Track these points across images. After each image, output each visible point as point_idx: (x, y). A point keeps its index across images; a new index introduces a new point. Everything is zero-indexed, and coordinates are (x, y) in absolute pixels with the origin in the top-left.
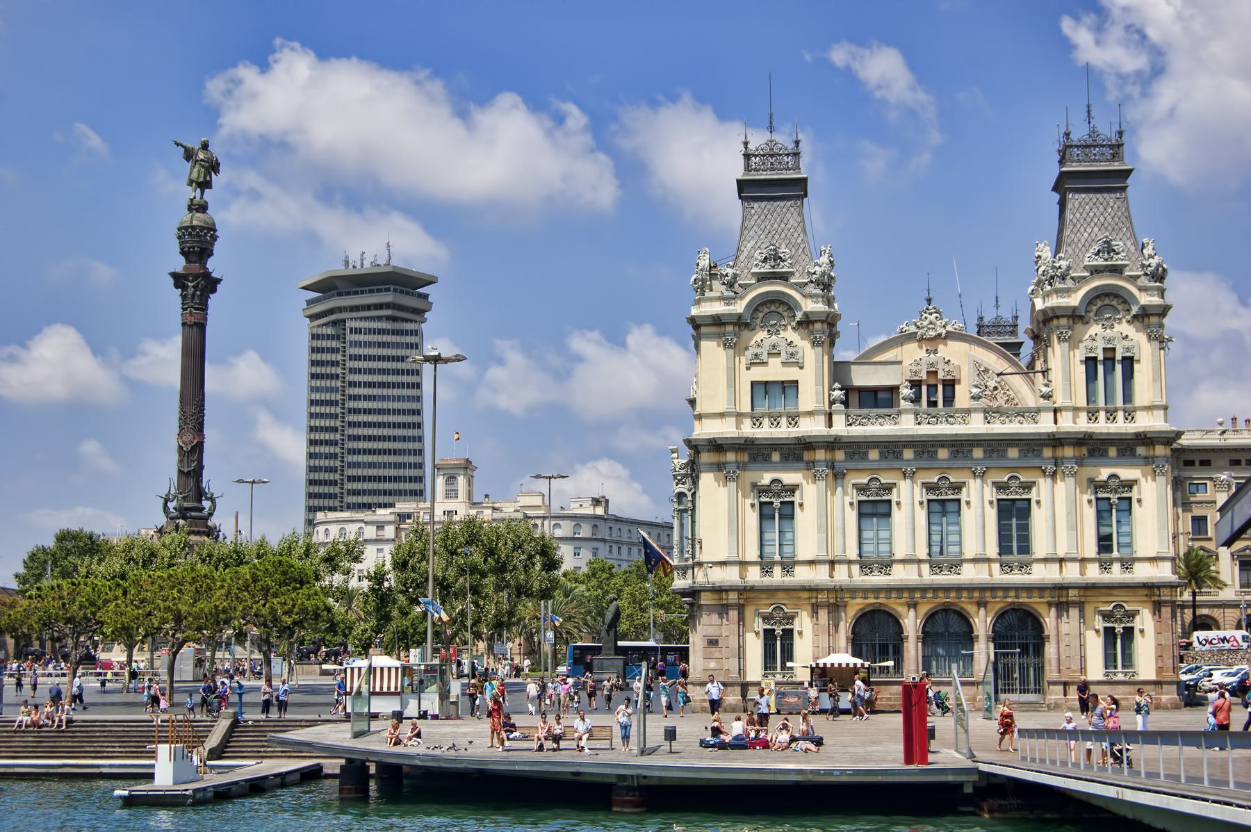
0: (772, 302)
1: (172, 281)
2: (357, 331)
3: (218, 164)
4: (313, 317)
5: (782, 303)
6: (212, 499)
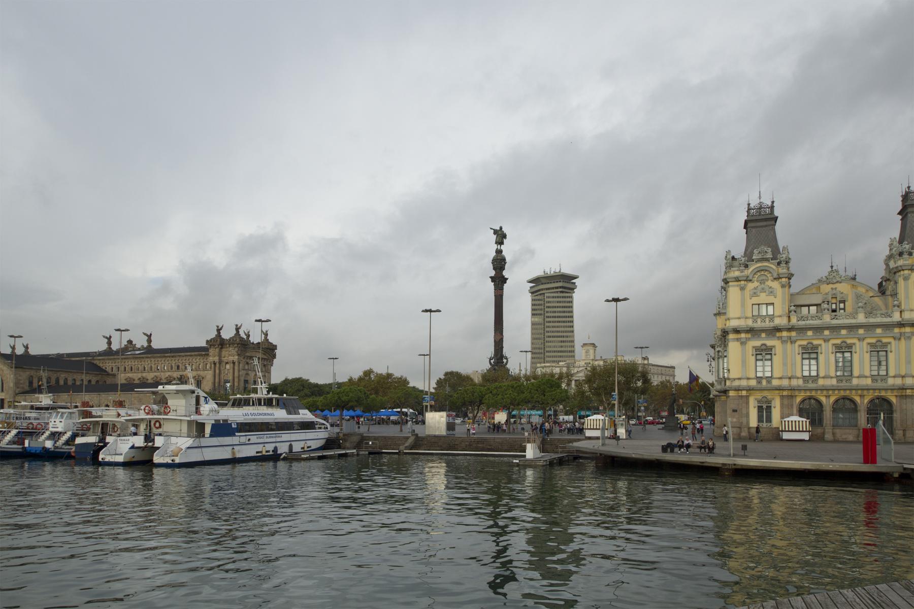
2: (549, 297)
4: (532, 293)
6: (506, 358)
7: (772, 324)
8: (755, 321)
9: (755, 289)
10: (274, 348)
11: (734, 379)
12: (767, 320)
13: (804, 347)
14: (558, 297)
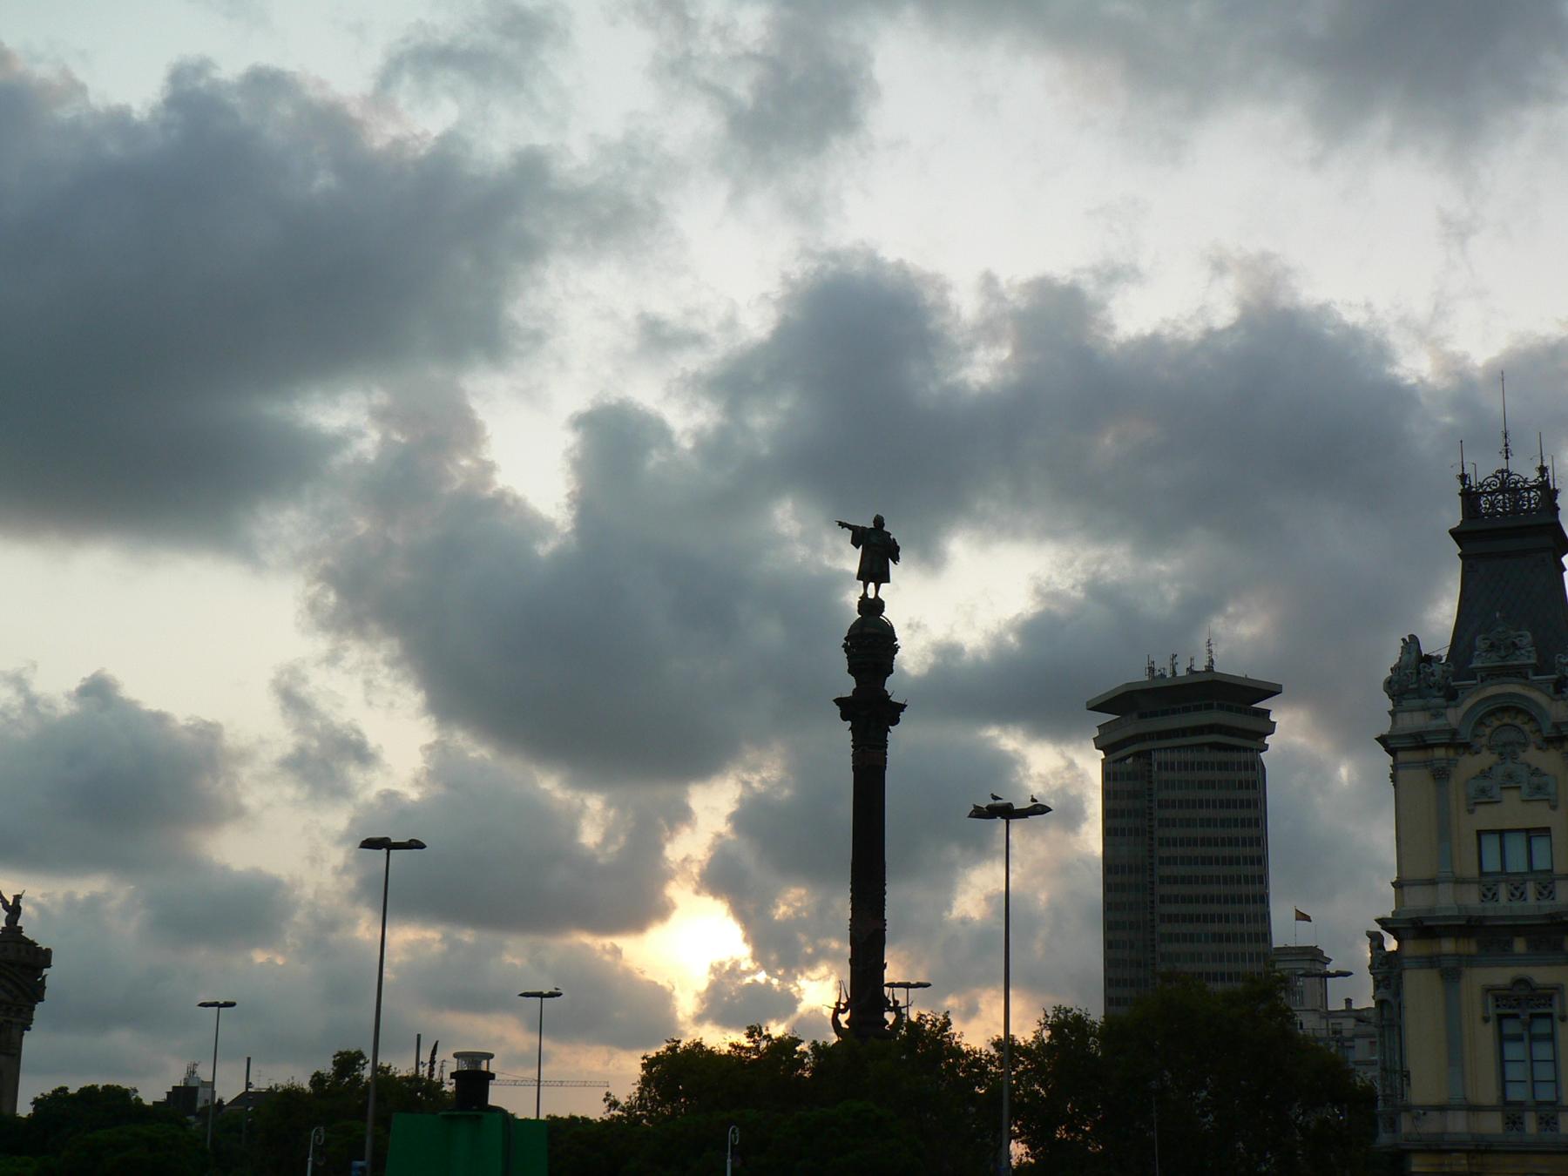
0: (1505, 710)
1: (837, 710)
2: (1168, 766)
3: (898, 549)
5: (1519, 711)
7: (1547, 906)
8: (1489, 894)
9: (1485, 774)
10: (42, 958)
11: (1427, 1109)
12: (1531, 889)
13: (1495, 994)
14: (1204, 766)
